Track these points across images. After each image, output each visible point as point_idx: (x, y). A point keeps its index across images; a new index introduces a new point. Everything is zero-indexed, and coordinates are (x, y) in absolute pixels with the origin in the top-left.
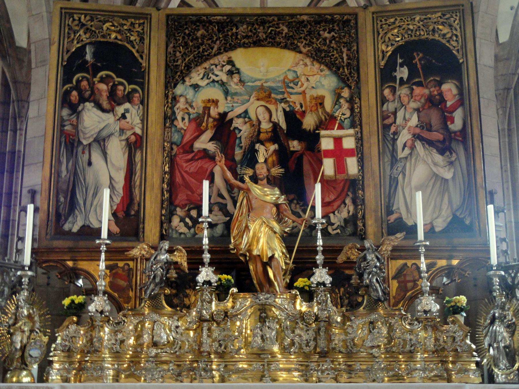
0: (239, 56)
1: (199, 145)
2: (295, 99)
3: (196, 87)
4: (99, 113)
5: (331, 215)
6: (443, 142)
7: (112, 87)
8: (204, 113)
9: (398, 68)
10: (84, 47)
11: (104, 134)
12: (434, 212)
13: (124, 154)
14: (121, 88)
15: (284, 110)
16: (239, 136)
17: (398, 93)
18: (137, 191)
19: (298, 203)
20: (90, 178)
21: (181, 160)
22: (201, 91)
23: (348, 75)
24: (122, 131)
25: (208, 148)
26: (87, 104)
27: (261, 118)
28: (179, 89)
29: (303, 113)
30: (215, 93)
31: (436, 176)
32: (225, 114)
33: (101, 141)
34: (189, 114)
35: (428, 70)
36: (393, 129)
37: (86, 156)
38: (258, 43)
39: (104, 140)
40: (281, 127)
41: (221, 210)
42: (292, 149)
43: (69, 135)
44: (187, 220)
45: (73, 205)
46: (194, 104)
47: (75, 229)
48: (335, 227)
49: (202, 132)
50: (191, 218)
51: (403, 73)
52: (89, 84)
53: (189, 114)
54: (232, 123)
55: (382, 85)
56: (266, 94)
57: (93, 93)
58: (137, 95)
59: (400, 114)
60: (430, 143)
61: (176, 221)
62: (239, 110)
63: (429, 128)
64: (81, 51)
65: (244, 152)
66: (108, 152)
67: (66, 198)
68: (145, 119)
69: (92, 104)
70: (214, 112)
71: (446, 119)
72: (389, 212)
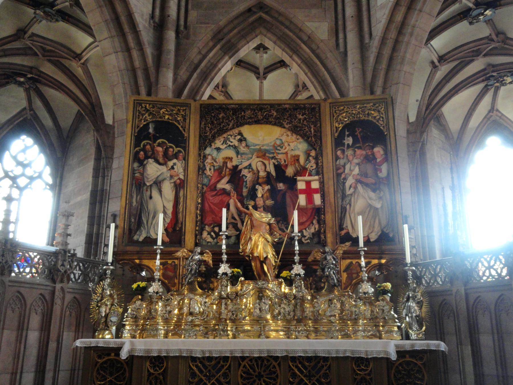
0: (246, 130)
1: (220, 186)
3: (218, 149)
4: (157, 165)
5: (304, 231)
6: (375, 184)
7: (165, 149)
8: (223, 165)
9: (346, 138)
10: (148, 124)
11: (160, 178)
12: (369, 229)
13: (173, 191)
14: (171, 150)
15: (274, 164)
16: (245, 180)
17: (346, 153)
18: (180, 215)
19: (283, 223)
20: (151, 207)
21: (209, 196)
22: (221, 152)
23: (315, 142)
24: (171, 177)
25: (226, 188)
26: (150, 160)
27: (259, 169)
28: (208, 151)
29: (286, 166)
30: (231, 153)
31: (370, 206)
32: (237, 166)
33: (158, 183)
34: (214, 166)
35: (365, 139)
36: (343, 176)
37: (149, 193)
38: (257, 122)
39: (160, 182)
40: (272, 175)
41: (234, 227)
42: (279, 189)
43: (138, 180)
44: (212, 234)
45: (139, 224)
46: (217, 160)
47: (141, 239)
48: (307, 238)
49: (222, 178)
50: (215, 232)
51: (349, 141)
52: (151, 147)
53: (214, 166)
54: (241, 172)
55: (336, 148)
56: (263, 154)
57: (153, 153)
58: (181, 154)
59: (348, 167)
60: (366, 185)
61: (205, 234)
62: (246, 164)
63: (366, 175)
64: (146, 126)
65: (249, 190)
66: (162, 190)
67: (135, 219)
68: (186, 169)
69: (153, 160)
70: (229, 165)
72: (341, 228)
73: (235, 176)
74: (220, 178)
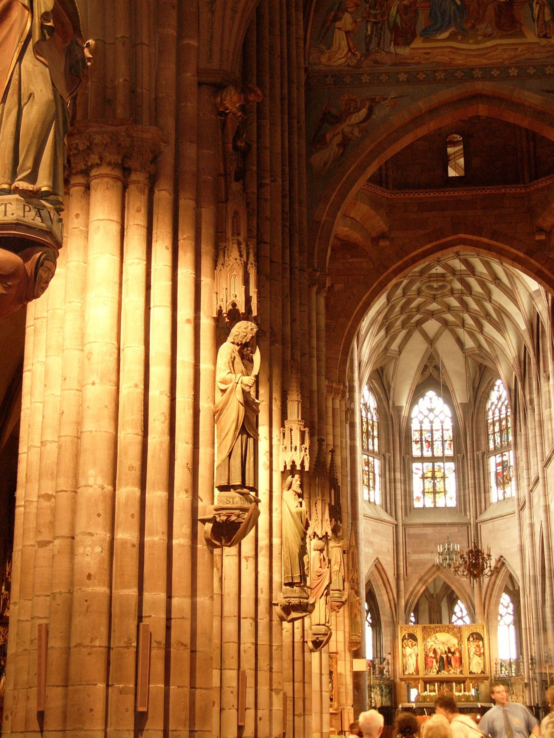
0: (438, 635)
2: (450, 645)
22: (431, 643)
33: (410, 655)
35: (477, 639)
38: (441, 632)
51: (471, 639)
56: (443, 643)
62: (438, 647)
64: (405, 636)
70: (433, 648)
73: (435, 651)
74: (430, 652)
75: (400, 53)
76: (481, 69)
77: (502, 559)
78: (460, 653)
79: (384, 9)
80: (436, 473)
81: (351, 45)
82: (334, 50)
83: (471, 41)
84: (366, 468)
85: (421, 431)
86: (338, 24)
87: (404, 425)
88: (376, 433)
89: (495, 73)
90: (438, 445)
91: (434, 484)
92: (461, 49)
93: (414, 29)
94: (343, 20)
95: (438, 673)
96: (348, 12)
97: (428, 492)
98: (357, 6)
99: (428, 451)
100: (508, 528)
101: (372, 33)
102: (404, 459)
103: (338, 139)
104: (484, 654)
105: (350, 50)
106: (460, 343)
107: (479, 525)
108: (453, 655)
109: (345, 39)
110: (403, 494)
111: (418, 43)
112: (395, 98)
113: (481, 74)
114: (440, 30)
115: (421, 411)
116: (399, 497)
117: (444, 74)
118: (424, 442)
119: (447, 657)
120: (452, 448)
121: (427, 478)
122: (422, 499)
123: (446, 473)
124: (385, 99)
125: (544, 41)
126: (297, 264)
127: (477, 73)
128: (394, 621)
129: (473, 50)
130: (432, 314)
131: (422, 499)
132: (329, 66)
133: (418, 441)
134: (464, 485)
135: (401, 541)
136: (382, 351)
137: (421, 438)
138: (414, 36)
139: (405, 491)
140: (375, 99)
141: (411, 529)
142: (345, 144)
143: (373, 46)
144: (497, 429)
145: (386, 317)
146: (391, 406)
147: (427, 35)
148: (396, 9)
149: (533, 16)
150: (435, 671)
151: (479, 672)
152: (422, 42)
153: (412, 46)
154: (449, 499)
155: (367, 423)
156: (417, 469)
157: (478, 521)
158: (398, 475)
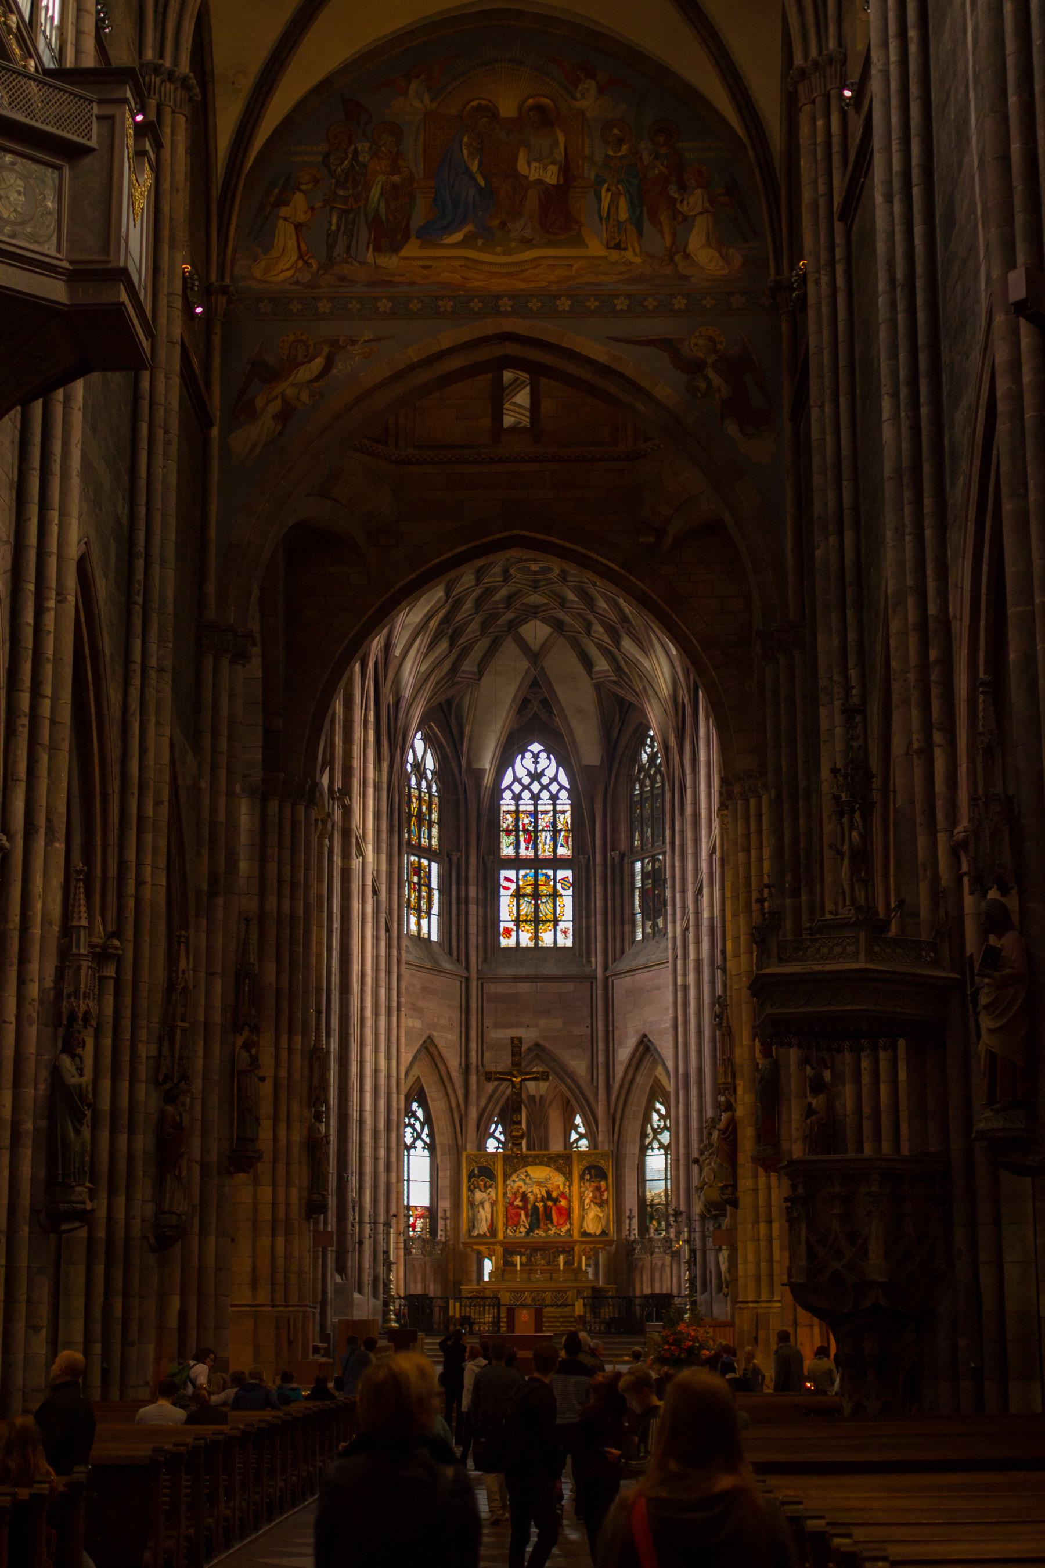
0: (529, 1169)
21: (510, 1208)
22: (516, 1183)
23: (568, 1176)
28: (508, 1182)
30: (521, 1183)
31: (597, 1216)
33: (482, 1203)
35: (597, 1176)
38: (536, 1164)
45: (474, 1227)
51: (588, 1177)
56: (539, 1184)
60: (596, 1203)
68: (497, 1194)
71: (602, 1195)
72: (581, 1227)
73: (524, 1197)
74: (516, 1198)
75: (384, 265)
76: (511, 297)
77: (645, 1040)
78: (569, 1201)
79: (360, 189)
80: (541, 888)
81: (303, 247)
82: (275, 255)
83: (499, 249)
84: (416, 879)
85: (517, 812)
86: (284, 211)
87: (486, 802)
88: (435, 816)
89: (534, 305)
90: (545, 837)
91: (537, 907)
92: (482, 263)
93: (408, 225)
94: (292, 204)
95: (528, 1233)
96: (300, 190)
97: (526, 921)
98: (316, 181)
99: (527, 848)
100: (658, 988)
101: (338, 229)
102: (484, 862)
103: (275, 407)
104: (607, 1200)
105: (301, 257)
106: (587, 663)
107: (610, 980)
108: (555, 1204)
109: (294, 237)
110: (480, 924)
111: (412, 249)
112: (370, 341)
113: (512, 306)
114: (449, 229)
115: (519, 775)
116: (473, 930)
117: (451, 303)
118: (521, 833)
119: (545, 1207)
120: (570, 843)
121: (525, 895)
122: (514, 934)
123: (559, 886)
124: (354, 342)
125: (615, 255)
126: (153, 662)
127: (506, 305)
128: (457, 1145)
129: (501, 265)
130: (534, 612)
131: (514, 934)
132: (266, 282)
133: (511, 831)
134: (588, 909)
135: (473, 1006)
136: (446, 675)
137: (517, 826)
138: (406, 237)
139: (485, 918)
140: (338, 341)
141: (492, 986)
142: (285, 415)
143: (339, 249)
144: (647, 812)
145: (446, 620)
146: (463, 769)
147: (428, 235)
148: (379, 190)
149: (599, 213)
150: (523, 1229)
151: (598, 1233)
152: (420, 248)
153: (403, 253)
154: (560, 936)
155: (420, 799)
156: (506, 879)
157: (608, 973)
158: (472, 891)
